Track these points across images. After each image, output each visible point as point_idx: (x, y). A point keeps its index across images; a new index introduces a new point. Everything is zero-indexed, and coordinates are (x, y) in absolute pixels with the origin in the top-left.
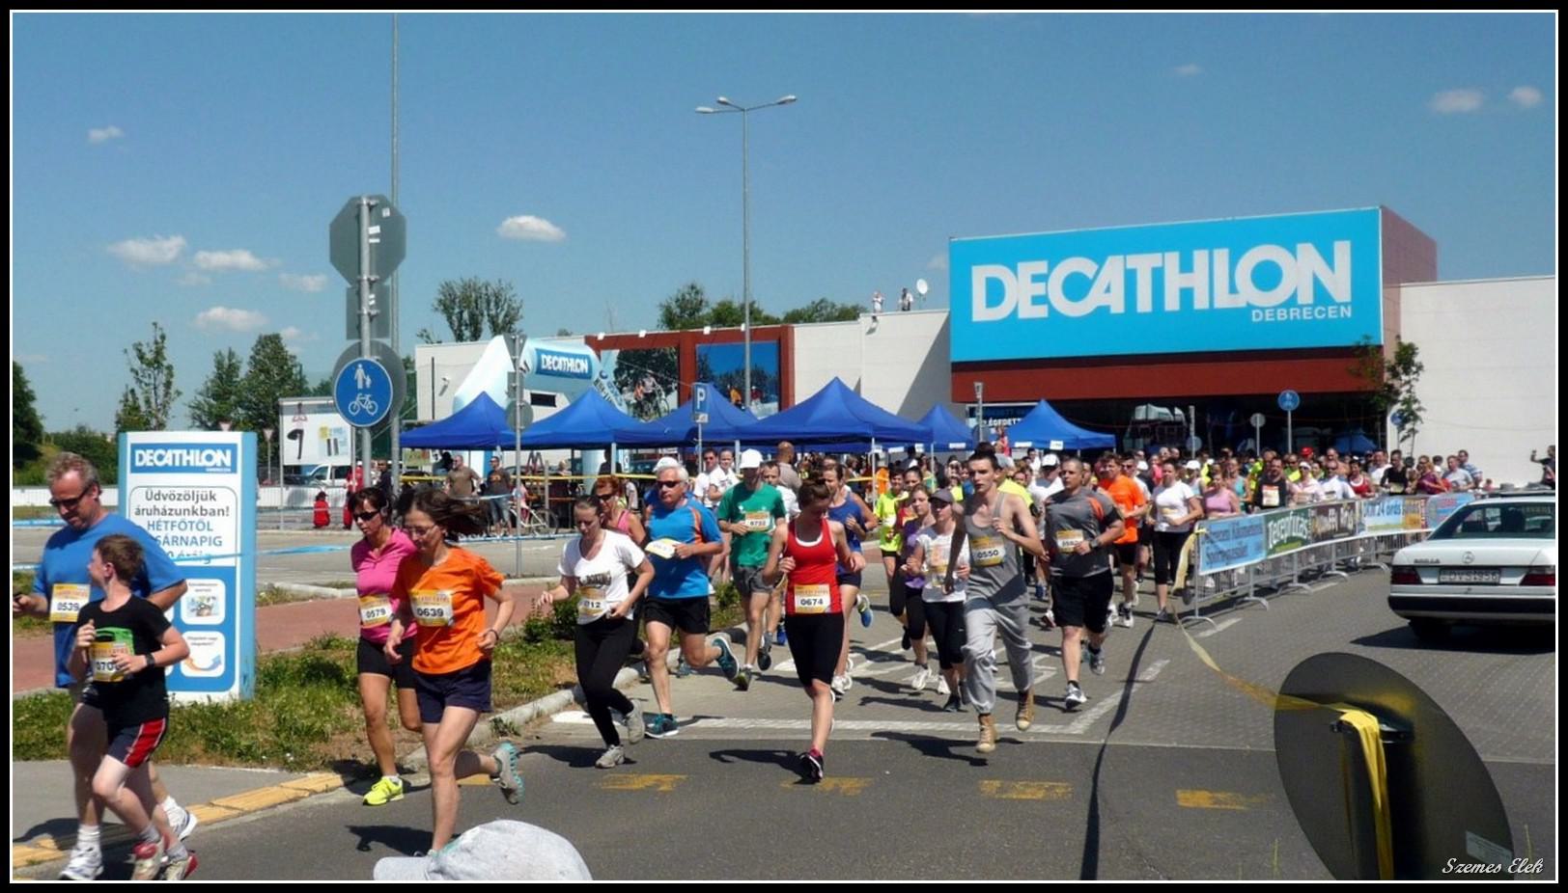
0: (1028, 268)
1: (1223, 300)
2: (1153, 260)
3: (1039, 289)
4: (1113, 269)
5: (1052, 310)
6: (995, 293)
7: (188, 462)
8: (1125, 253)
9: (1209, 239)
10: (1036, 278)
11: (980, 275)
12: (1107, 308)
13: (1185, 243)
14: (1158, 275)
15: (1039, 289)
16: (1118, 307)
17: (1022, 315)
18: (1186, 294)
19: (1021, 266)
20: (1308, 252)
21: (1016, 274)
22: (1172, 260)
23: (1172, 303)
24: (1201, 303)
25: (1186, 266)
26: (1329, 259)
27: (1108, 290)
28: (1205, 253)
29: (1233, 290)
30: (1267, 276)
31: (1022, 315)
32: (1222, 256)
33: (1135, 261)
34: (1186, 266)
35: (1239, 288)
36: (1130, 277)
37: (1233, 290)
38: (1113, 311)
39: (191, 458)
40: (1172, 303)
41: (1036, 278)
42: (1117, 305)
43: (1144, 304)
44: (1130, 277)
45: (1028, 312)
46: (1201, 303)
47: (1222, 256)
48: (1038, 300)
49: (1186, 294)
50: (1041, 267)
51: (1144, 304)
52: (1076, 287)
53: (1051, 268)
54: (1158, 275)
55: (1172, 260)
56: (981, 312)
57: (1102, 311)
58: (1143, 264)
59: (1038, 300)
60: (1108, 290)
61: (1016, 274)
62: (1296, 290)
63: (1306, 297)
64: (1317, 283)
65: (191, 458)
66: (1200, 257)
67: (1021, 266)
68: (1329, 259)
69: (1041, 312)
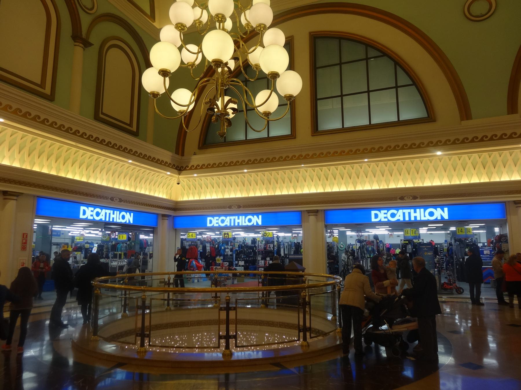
0: (383, 212)
1: (423, 218)
2: (409, 211)
3: (385, 215)
4: (401, 212)
5: (388, 219)
6: (376, 216)
7: (238, 223)
8: (403, 209)
9: (420, 207)
10: (385, 214)
11: (373, 212)
13: (415, 208)
14: (409, 213)
15: (385, 215)
17: (382, 221)
18: (415, 217)
19: (381, 211)
20: (439, 209)
21: (380, 212)
24: (418, 219)
25: (415, 212)
26: (443, 211)
27: (399, 216)
28: (419, 209)
29: (425, 216)
31: (382, 221)
32: (422, 210)
33: (405, 211)
34: (415, 212)
35: (426, 216)
36: (404, 214)
37: (425, 216)
38: (401, 220)
39: (240, 221)
41: (385, 214)
42: (402, 219)
44: (404, 214)
45: (383, 220)
46: (418, 219)
47: (422, 210)
48: (385, 218)
49: (415, 217)
50: (386, 211)
52: (393, 215)
53: (388, 212)
54: (409, 213)
55: (412, 211)
57: (399, 220)
58: (407, 211)
59: (385, 218)
60: (399, 216)
61: (380, 212)
62: (437, 217)
63: (439, 218)
64: (441, 216)
65: (240, 221)
66: (418, 210)
67: (381, 211)
68: (443, 211)
69: (386, 220)
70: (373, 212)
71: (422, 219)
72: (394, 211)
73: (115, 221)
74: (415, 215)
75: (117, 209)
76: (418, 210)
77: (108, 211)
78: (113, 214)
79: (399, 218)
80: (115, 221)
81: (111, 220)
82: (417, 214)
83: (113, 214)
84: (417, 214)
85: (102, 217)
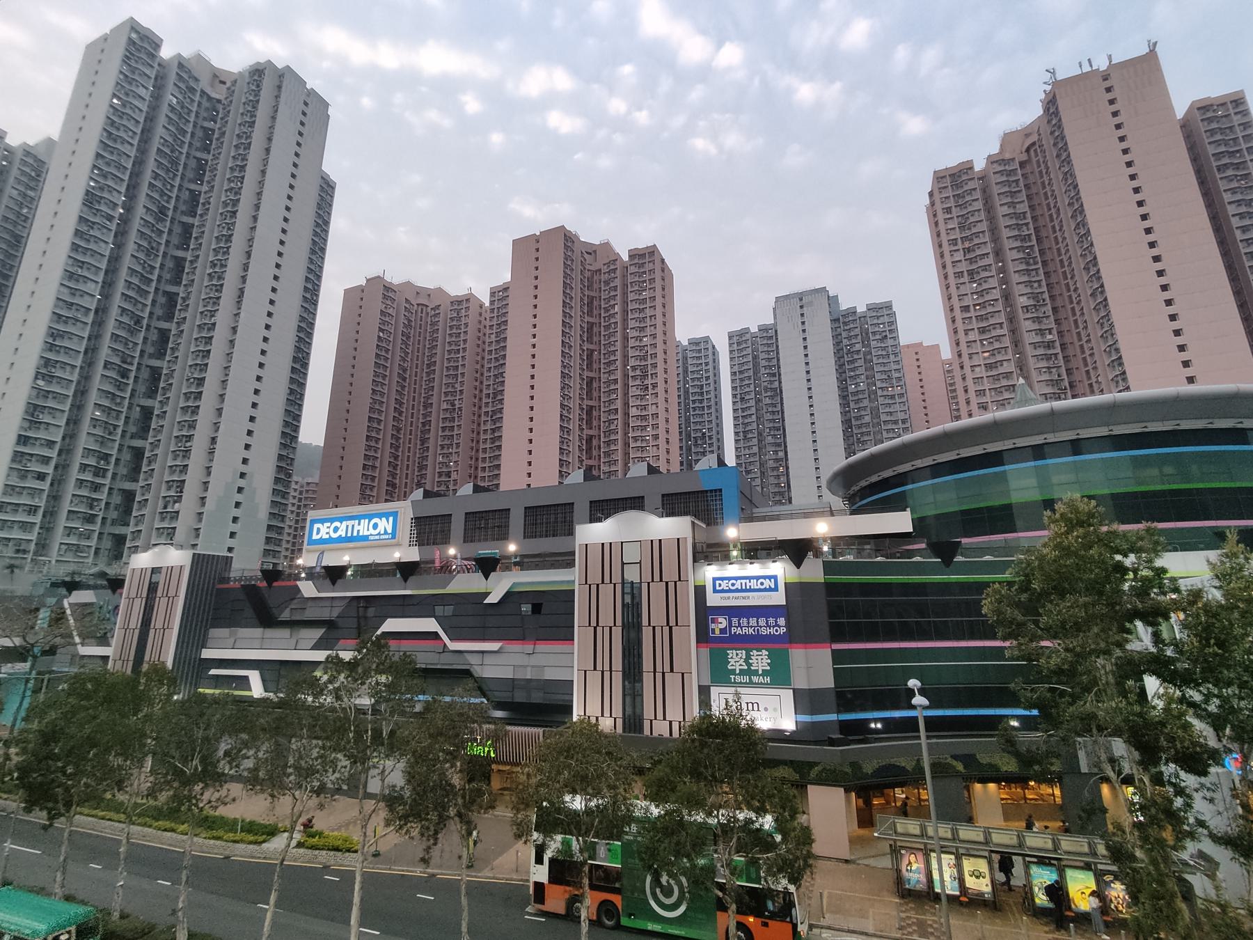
6: (720, 585)
11: (718, 582)
30: (762, 584)
52: (733, 585)
56: (718, 588)
58: (743, 581)
70: (718, 582)
72: (734, 581)
73: (361, 534)
75: (364, 517)
77: (350, 523)
78: (359, 524)
80: (361, 534)
81: (355, 534)
82: (751, 584)
83: (359, 524)
84: (751, 584)
85: (342, 533)
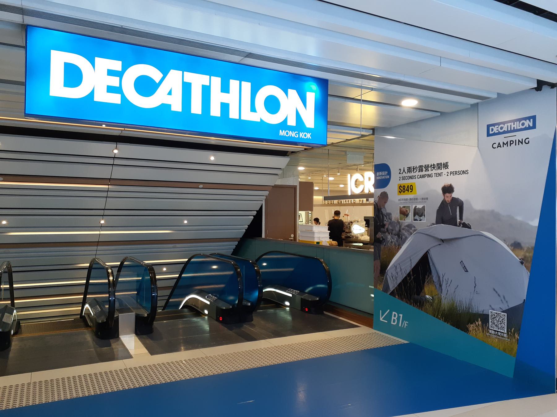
1: (247, 116)
2: (204, 79)
12: (170, 105)
14: (206, 91)
16: (177, 106)
18: (225, 107)
22: (216, 82)
23: (215, 111)
24: (233, 114)
25: (225, 89)
27: (170, 93)
29: (253, 109)
33: (190, 77)
34: (225, 89)
36: (187, 88)
37: (253, 109)
40: (215, 111)
42: (177, 106)
43: (196, 108)
44: (187, 88)
46: (233, 114)
49: (225, 107)
51: (196, 108)
54: (206, 91)
55: (216, 82)
57: (166, 107)
60: (170, 93)
66: (234, 84)
71: (243, 118)
74: (225, 98)
76: (234, 84)
79: (167, 100)
82: (231, 98)
84: (231, 98)
